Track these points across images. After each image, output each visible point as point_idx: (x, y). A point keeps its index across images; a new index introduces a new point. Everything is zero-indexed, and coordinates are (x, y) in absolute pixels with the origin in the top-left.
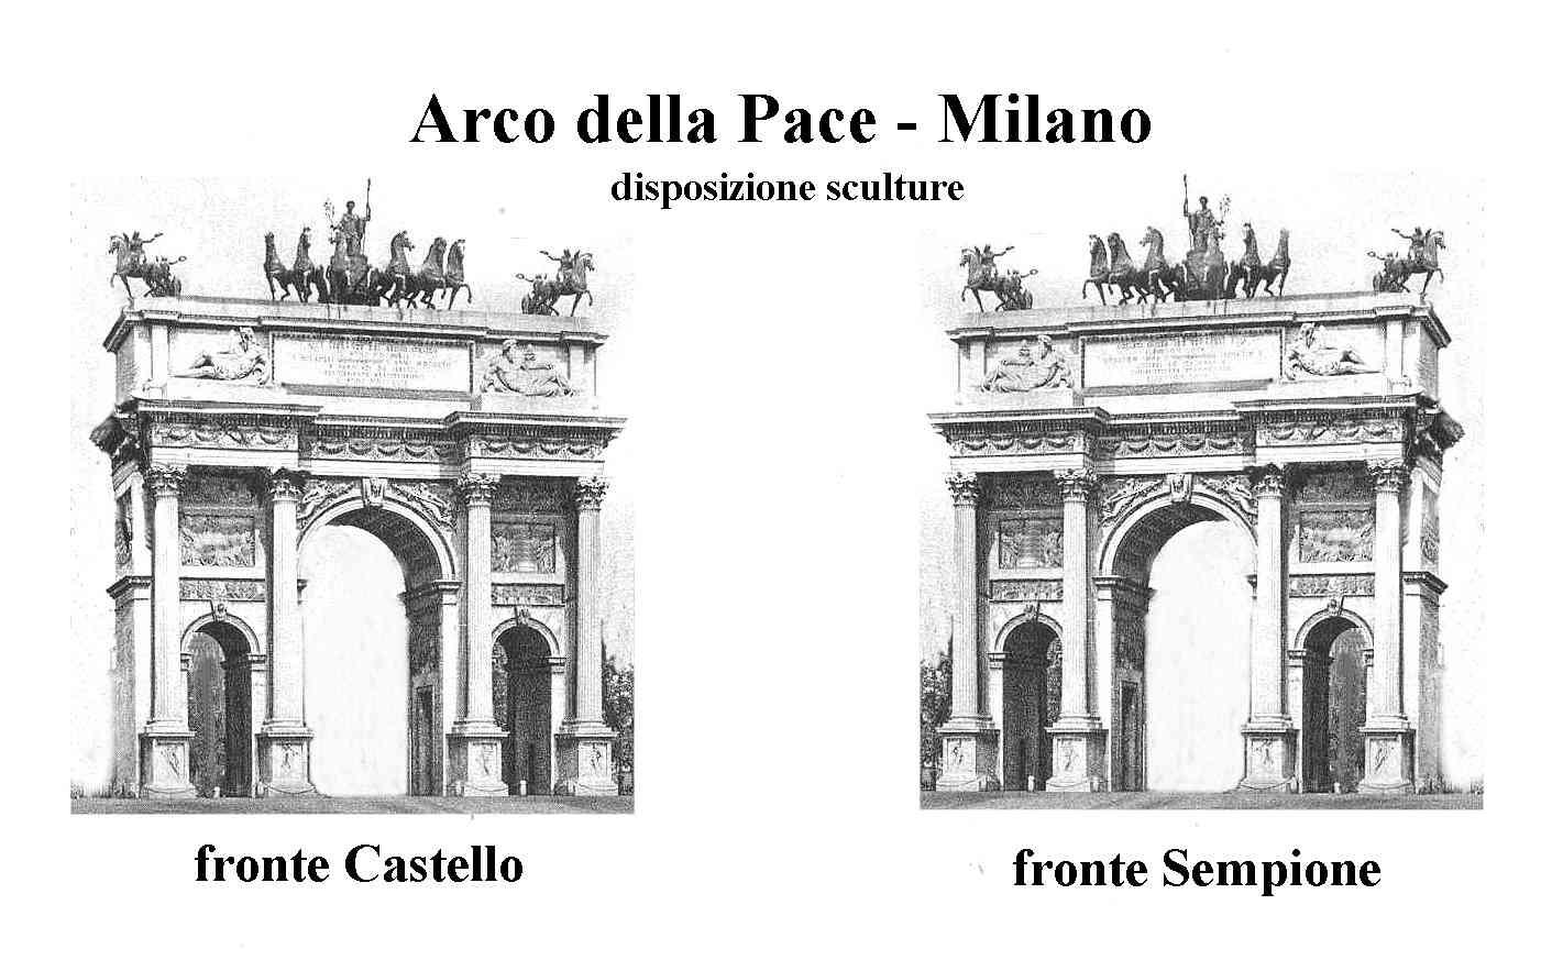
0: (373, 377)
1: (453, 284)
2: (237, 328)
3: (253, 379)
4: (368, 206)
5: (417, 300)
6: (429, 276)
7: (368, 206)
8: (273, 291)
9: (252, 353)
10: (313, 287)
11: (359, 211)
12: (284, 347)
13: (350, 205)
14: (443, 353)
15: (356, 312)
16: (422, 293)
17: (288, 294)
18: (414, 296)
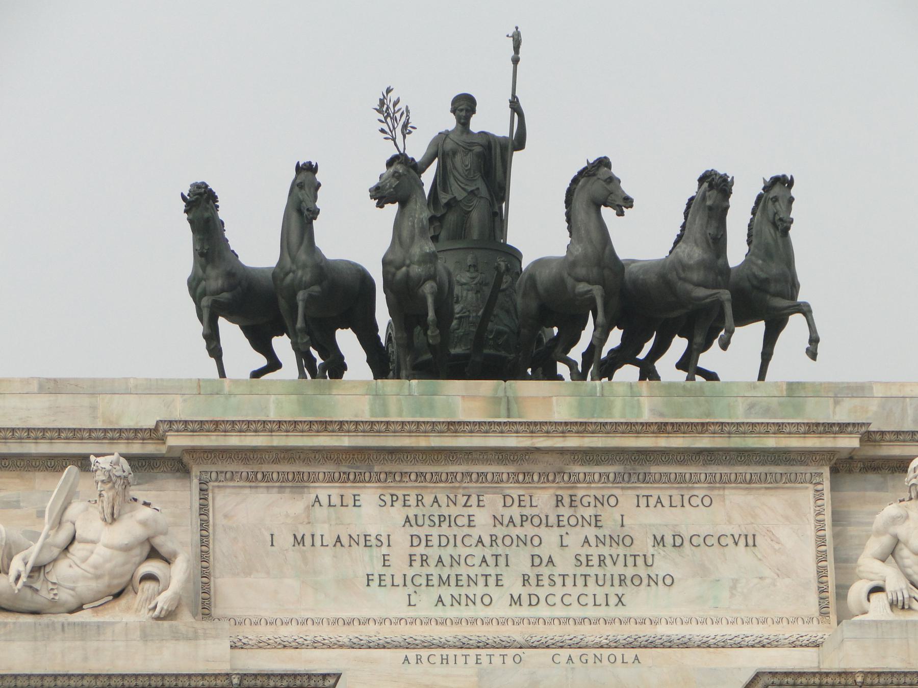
0: (517, 589)
1: (767, 296)
2: (83, 462)
3: (129, 615)
4: (515, 106)
5: (667, 365)
6: (680, 285)
7: (515, 106)
8: (215, 350)
9: (129, 529)
10: (347, 341)
11: (491, 121)
12: (251, 511)
13: (464, 106)
14: (735, 507)
15: (464, 399)
16: (679, 345)
17: (274, 364)
18: (659, 350)
